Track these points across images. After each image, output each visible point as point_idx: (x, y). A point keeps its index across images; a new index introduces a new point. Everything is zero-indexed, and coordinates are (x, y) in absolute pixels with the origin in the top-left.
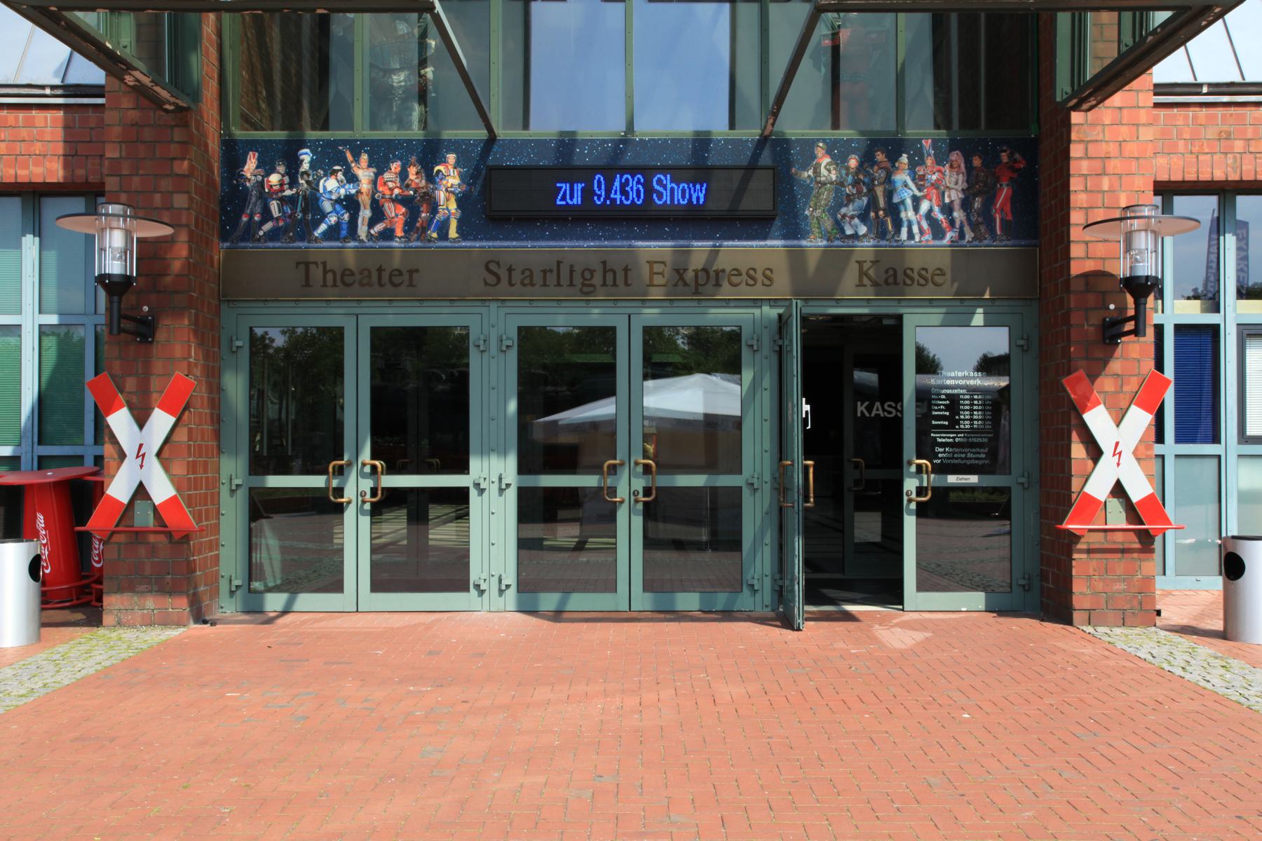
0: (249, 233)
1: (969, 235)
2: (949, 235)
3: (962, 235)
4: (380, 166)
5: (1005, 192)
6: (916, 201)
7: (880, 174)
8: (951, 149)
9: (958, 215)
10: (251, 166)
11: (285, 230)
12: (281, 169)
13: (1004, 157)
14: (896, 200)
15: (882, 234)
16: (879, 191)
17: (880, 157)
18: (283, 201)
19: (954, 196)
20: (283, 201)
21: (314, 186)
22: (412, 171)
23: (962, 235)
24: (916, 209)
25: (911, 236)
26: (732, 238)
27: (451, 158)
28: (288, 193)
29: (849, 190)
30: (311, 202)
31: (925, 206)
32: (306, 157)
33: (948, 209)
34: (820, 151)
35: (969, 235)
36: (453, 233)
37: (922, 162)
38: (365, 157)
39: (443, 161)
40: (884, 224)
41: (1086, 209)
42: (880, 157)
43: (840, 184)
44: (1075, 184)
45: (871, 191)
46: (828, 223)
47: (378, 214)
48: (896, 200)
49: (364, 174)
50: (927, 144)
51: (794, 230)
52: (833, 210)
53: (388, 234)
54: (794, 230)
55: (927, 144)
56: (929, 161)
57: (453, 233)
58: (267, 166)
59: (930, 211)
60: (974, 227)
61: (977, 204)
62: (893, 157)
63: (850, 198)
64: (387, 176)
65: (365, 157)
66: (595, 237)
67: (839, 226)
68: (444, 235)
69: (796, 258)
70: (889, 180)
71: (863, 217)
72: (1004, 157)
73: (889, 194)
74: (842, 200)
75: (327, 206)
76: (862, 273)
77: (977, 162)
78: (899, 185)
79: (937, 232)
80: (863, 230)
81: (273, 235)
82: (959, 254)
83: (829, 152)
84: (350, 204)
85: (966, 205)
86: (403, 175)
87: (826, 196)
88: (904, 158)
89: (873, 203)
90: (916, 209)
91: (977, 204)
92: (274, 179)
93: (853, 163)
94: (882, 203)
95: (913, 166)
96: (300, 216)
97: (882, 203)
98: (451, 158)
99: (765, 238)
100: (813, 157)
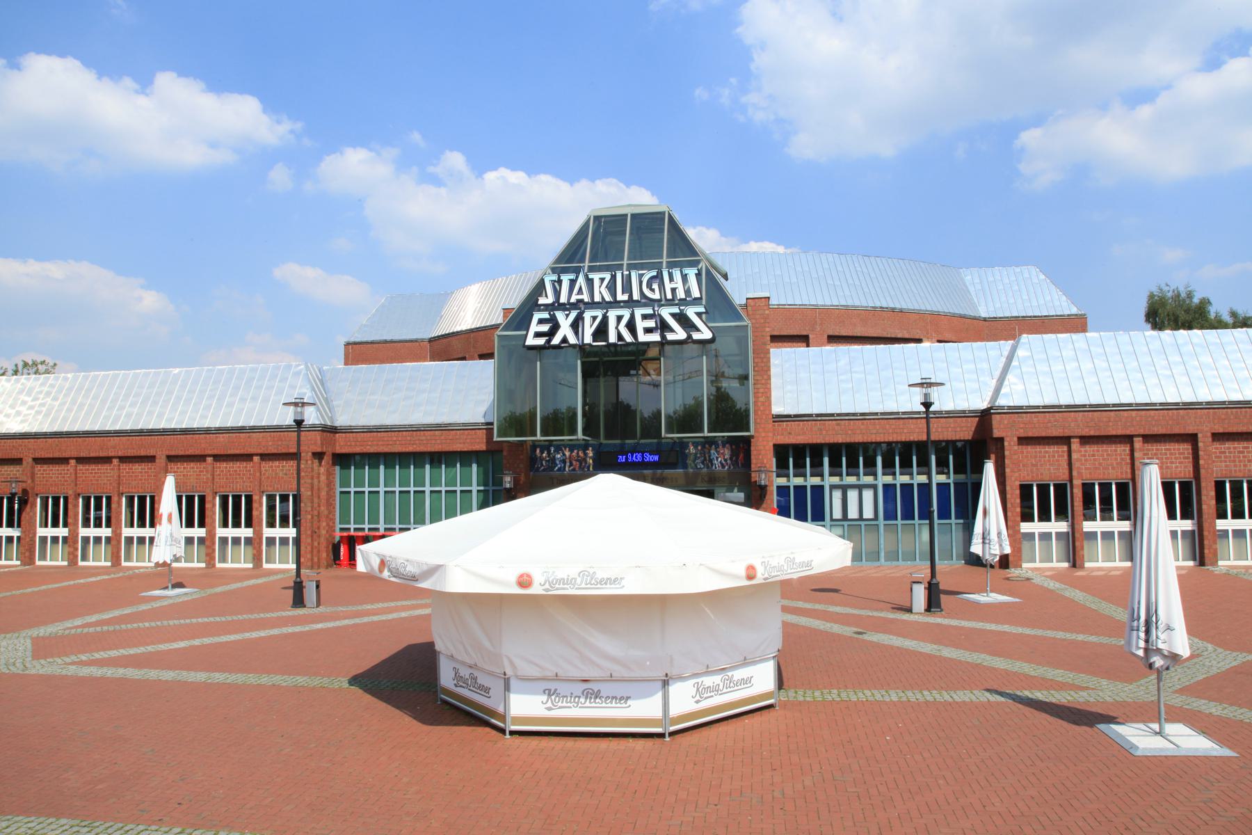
0: (537, 470)
1: (732, 467)
2: (727, 467)
3: (730, 467)
4: (571, 451)
5: (741, 455)
6: (717, 458)
7: (706, 451)
8: (727, 443)
9: (729, 461)
10: (538, 451)
11: (546, 469)
12: (546, 452)
13: (741, 445)
14: (711, 458)
15: (708, 467)
16: (707, 455)
17: (707, 446)
18: (546, 461)
19: (727, 456)
20: (546, 461)
21: (555, 456)
22: (580, 452)
23: (730, 467)
24: (717, 460)
25: (716, 468)
26: (666, 469)
27: (590, 448)
28: (548, 459)
29: (698, 455)
30: (553, 460)
31: (719, 459)
32: (552, 449)
33: (726, 460)
34: (690, 444)
35: (732, 467)
36: (591, 469)
37: (718, 447)
38: (567, 449)
39: (588, 449)
40: (708, 465)
41: (756, 464)
42: (707, 446)
43: (696, 454)
44: (752, 457)
45: (705, 455)
46: (693, 465)
47: (571, 464)
48: (711, 458)
49: (567, 454)
50: (720, 442)
51: (685, 466)
52: (694, 461)
53: (574, 470)
54: (685, 466)
55: (720, 442)
56: (721, 447)
57: (591, 469)
58: (542, 452)
59: (721, 461)
60: (733, 465)
61: (734, 458)
62: (711, 446)
63: (699, 458)
64: (574, 454)
65: (567, 449)
66: (629, 470)
67: (696, 466)
68: (589, 469)
69: (686, 474)
70: (709, 452)
71: (703, 463)
72: (741, 445)
73: (710, 456)
74: (696, 458)
75: (558, 462)
76: (703, 479)
77: (734, 447)
78: (712, 454)
79: (723, 466)
80: (702, 466)
81: (544, 470)
82: (730, 473)
83: (693, 445)
84: (564, 462)
85: (731, 459)
86: (578, 453)
87: (692, 457)
88: (713, 446)
89: (705, 459)
90: (717, 460)
91: (734, 458)
92: (544, 455)
93: (699, 448)
94: (707, 458)
95: (716, 448)
96: (550, 465)
97: (707, 458)
98: (590, 448)
99: (675, 469)
100: (688, 446)
